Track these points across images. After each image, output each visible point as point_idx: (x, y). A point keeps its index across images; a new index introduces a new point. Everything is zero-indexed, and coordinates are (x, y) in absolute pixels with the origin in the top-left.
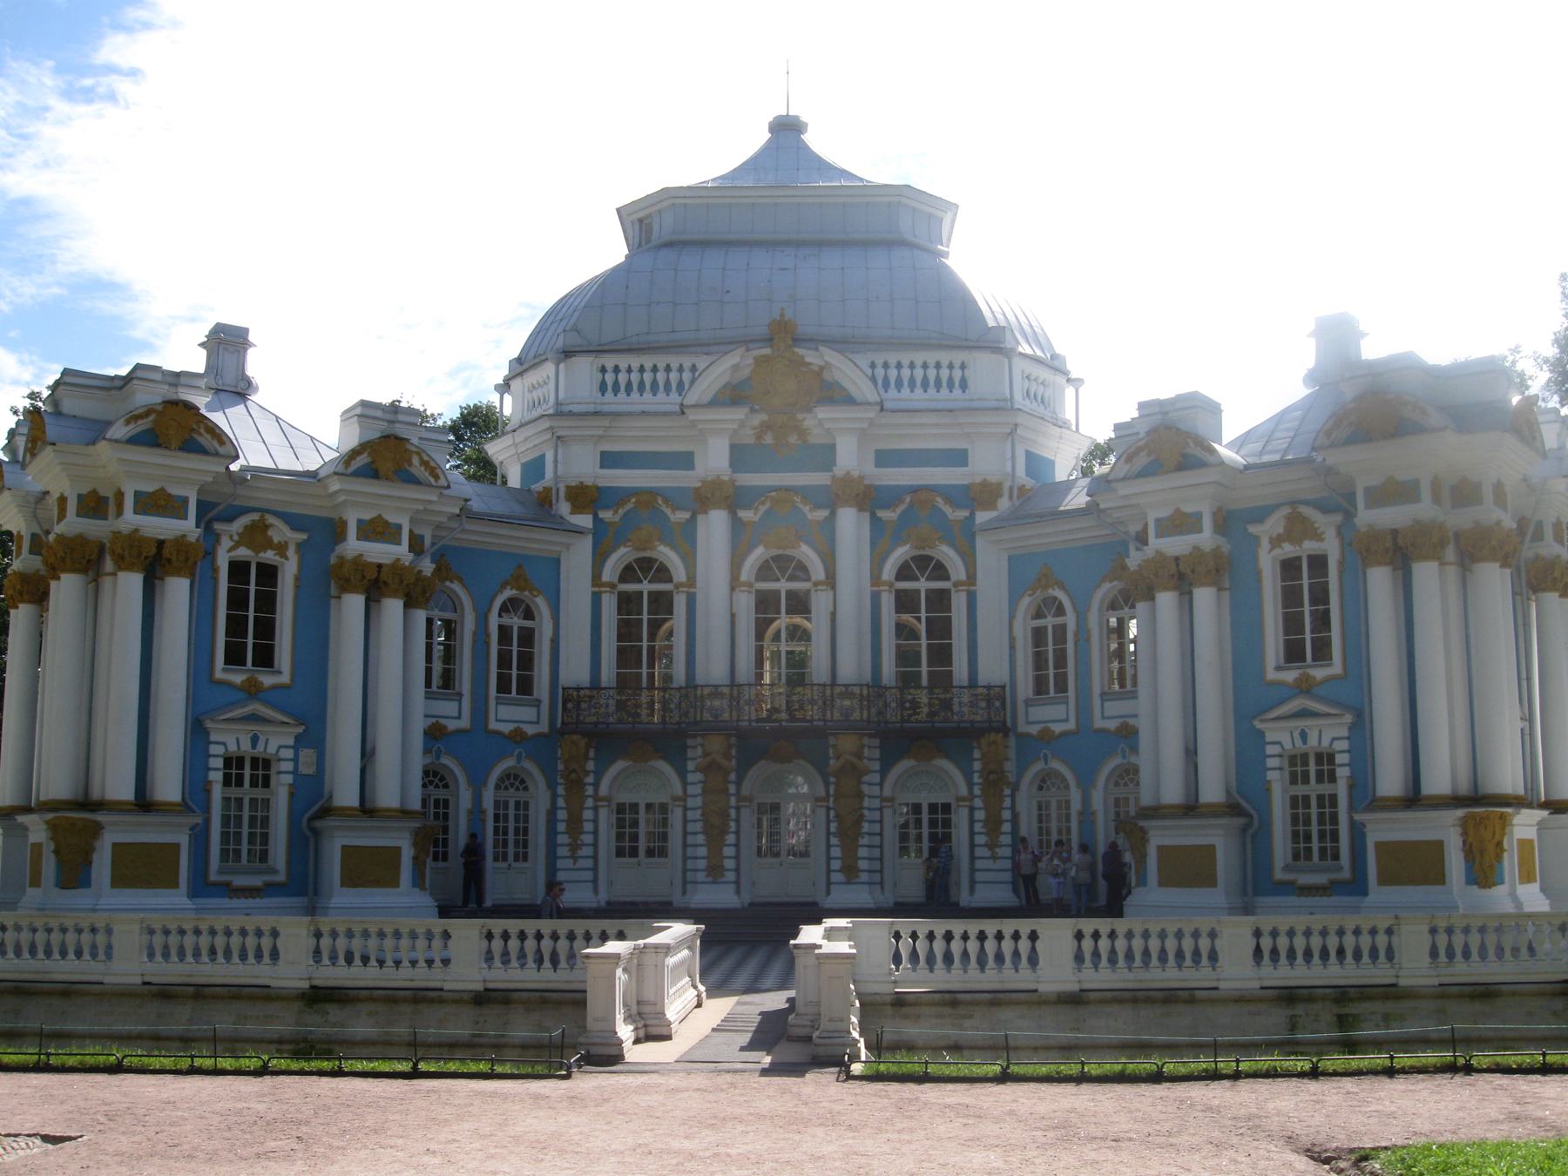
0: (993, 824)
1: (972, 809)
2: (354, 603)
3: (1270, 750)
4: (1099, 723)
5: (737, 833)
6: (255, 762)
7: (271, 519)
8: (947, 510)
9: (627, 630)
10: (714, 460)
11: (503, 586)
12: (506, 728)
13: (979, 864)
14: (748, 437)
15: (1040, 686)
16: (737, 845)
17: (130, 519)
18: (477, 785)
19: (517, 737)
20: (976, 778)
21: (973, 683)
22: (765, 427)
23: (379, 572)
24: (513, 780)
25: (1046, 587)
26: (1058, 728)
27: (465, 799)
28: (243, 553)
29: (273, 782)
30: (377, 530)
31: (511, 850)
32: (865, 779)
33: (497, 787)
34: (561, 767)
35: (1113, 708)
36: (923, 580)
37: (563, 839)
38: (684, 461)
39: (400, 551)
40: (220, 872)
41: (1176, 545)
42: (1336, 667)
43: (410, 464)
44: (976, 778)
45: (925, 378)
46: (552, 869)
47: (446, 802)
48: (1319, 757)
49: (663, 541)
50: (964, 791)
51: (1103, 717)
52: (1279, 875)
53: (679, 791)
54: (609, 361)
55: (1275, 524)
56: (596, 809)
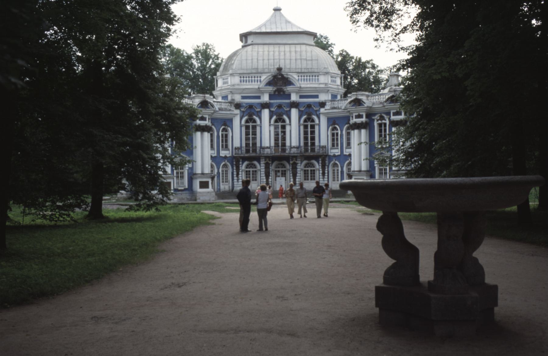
0: (324, 174)
4: (345, 153)
5: (272, 176)
8: (314, 108)
10: (265, 98)
12: (223, 155)
15: (333, 145)
16: (272, 179)
19: (225, 157)
20: (320, 164)
21: (320, 146)
22: (275, 91)
25: (334, 125)
26: (337, 154)
29: (184, 168)
31: (224, 180)
32: (298, 165)
33: (222, 168)
35: (348, 150)
37: (235, 178)
41: (359, 120)
43: (208, 105)
51: (346, 152)
55: (377, 117)
56: (242, 172)
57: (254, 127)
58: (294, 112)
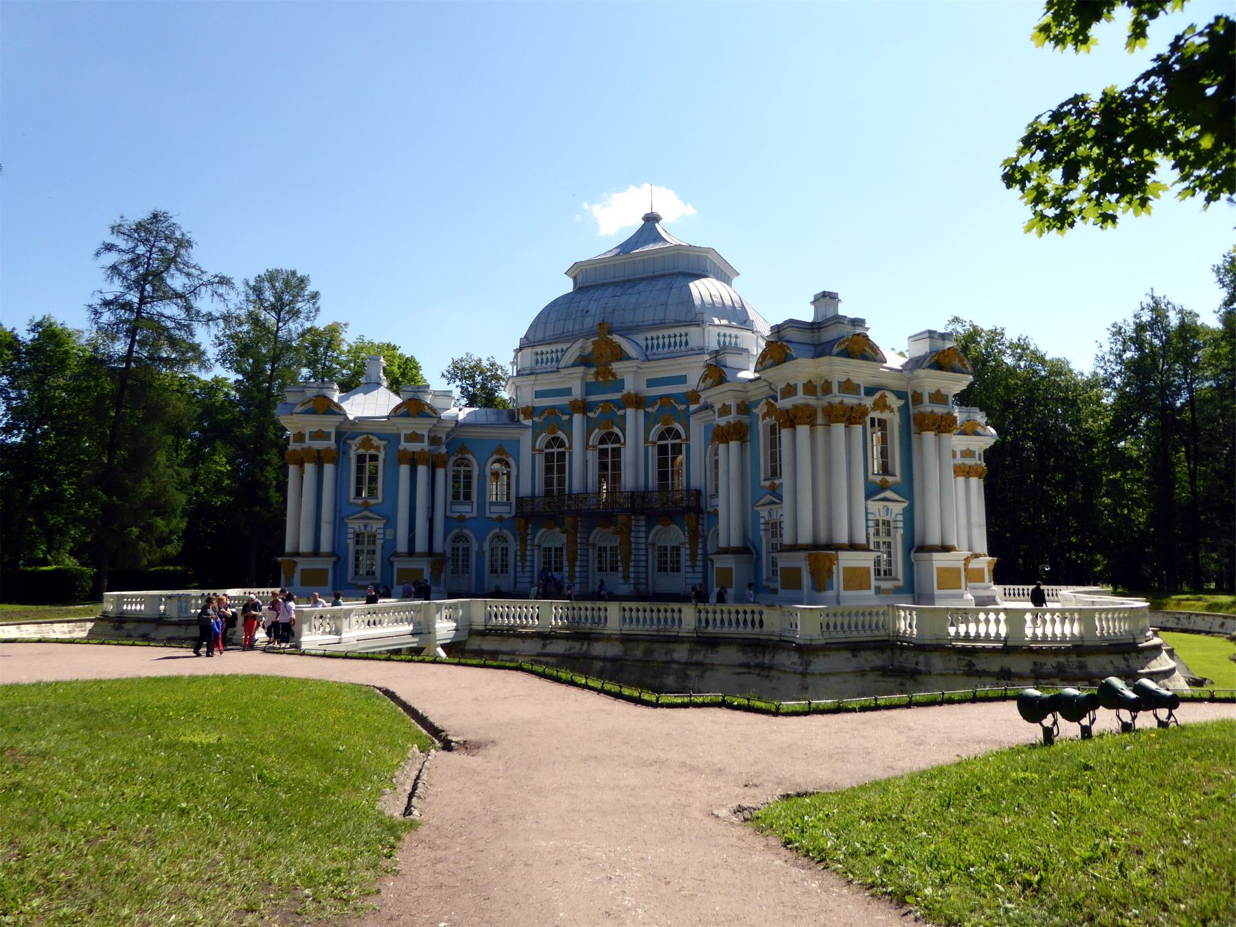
0: (693, 556)
2: (404, 470)
7: (371, 437)
9: (549, 469)
11: (492, 454)
12: (494, 516)
14: (591, 379)
18: (480, 541)
19: (500, 519)
21: (688, 490)
22: (597, 374)
24: (498, 537)
27: (474, 547)
28: (362, 451)
37: (519, 564)
38: (567, 392)
39: (425, 446)
40: (353, 579)
45: (681, 341)
46: (516, 577)
47: (468, 549)
49: (559, 429)
54: (538, 349)
56: (532, 550)
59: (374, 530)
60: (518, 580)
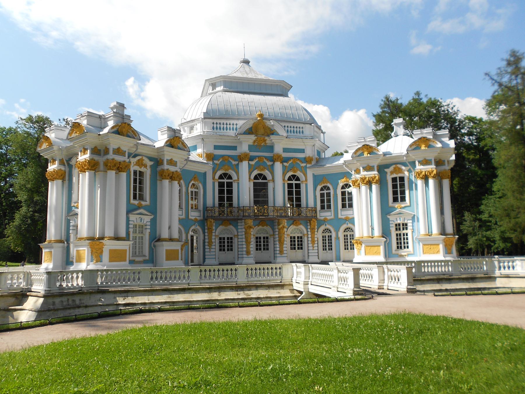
0: (313, 242)
1: (308, 238)
3: (391, 222)
4: (340, 216)
6: (139, 225)
7: (144, 158)
9: (221, 192)
10: (244, 148)
12: (193, 218)
13: (310, 251)
15: (323, 207)
17: (111, 156)
19: (196, 221)
20: (309, 230)
23: (173, 174)
26: (329, 218)
30: (171, 162)
34: (206, 227)
36: (294, 181)
37: (207, 247)
38: (234, 148)
42: (408, 204)
44: (309, 230)
48: (403, 224)
50: (305, 232)
52: (394, 252)
53: (236, 234)
54: (215, 121)
57: (230, 185)
58: (278, 166)
59: (145, 222)
60: (206, 257)
